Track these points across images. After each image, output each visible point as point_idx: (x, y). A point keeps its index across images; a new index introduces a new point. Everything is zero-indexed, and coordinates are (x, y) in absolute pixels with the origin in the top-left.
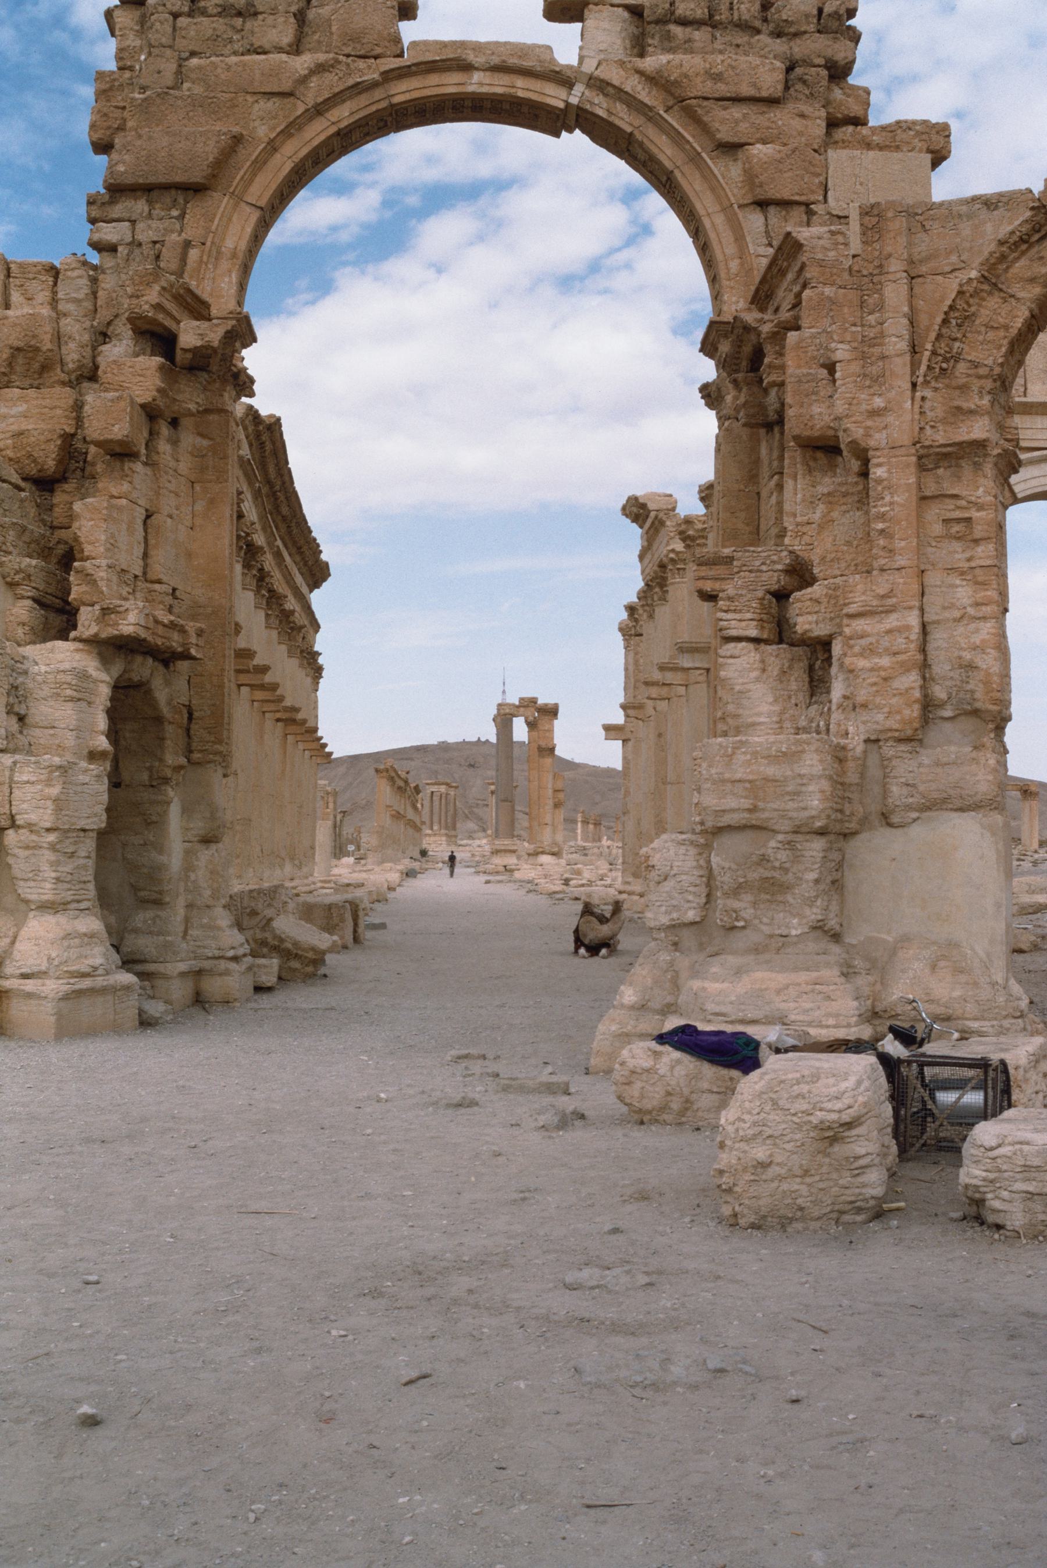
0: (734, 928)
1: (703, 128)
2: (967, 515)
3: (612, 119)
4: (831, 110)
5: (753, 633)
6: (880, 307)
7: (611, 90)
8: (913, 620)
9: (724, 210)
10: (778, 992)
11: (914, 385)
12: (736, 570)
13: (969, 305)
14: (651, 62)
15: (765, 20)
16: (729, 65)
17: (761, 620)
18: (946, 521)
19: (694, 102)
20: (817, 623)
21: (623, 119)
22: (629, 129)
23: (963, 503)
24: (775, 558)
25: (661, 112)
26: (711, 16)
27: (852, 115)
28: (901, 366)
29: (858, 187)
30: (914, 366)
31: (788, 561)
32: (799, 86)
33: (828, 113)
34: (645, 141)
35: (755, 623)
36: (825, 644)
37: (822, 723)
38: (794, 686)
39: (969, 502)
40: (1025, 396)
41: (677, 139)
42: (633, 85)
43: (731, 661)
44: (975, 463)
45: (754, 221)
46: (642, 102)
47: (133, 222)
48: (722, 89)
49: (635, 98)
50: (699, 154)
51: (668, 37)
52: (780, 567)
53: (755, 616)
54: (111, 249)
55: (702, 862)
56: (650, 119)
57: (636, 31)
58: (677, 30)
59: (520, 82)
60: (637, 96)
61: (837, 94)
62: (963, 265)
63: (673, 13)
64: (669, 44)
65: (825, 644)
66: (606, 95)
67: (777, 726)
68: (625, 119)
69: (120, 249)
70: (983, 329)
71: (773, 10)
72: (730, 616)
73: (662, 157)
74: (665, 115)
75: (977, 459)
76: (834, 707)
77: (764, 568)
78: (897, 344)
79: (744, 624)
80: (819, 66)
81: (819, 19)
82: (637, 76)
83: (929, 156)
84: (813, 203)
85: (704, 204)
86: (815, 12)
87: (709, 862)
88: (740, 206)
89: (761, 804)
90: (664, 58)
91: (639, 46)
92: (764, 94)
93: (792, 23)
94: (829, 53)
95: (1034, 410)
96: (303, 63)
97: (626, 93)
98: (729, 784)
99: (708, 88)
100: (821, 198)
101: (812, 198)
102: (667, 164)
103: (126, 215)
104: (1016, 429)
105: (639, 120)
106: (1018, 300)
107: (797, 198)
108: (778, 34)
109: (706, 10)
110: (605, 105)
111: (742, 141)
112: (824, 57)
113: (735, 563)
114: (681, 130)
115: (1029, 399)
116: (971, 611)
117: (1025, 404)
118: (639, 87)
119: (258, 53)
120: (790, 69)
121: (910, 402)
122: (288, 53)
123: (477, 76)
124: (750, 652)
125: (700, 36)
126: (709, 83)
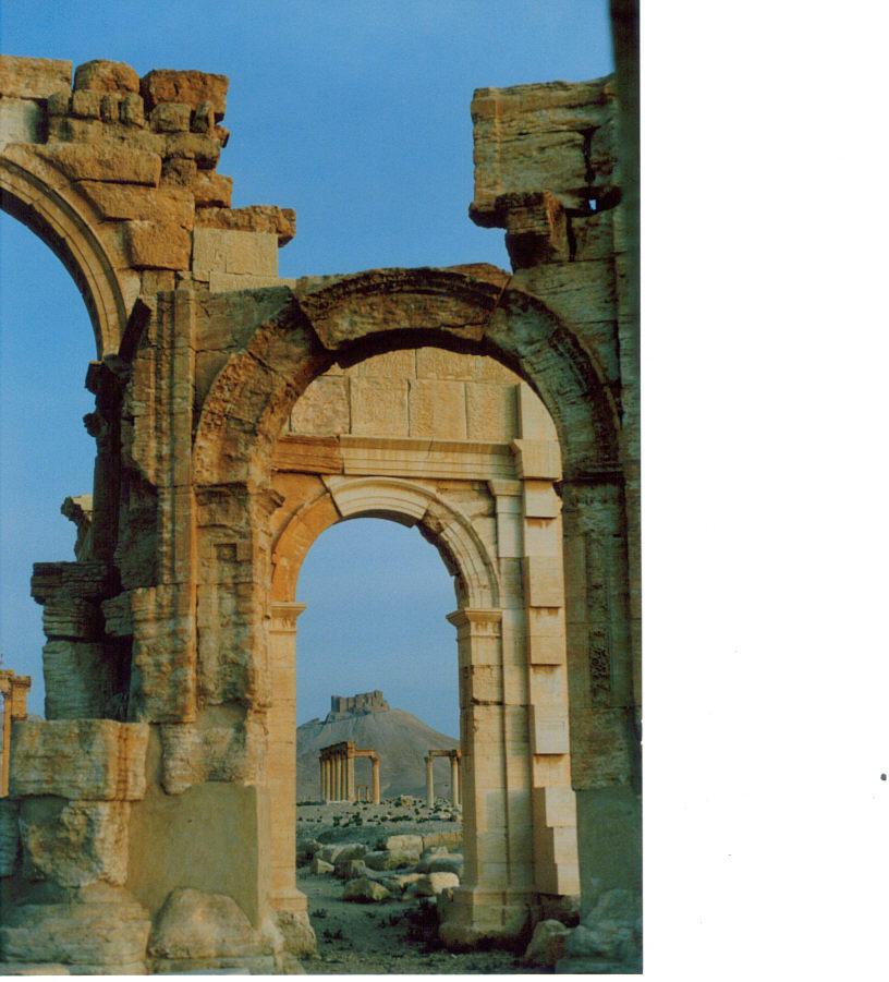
0: (36, 881)
1: (93, 205)
2: (233, 541)
3: (15, 192)
4: (199, 194)
5: (71, 633)
7: (16, 170)
9: (106, 273)
10: (64, 935)
12: (64, 580)
13: (239, 376)
15: (148, 119)
16: (115, 154)
17: (79, 622)
18: (218, 546)
19: (83, 183)
20: (120, 625)
21: (23, 193)
22: (29, 202)
23: (231, 532)
24: (95, 571)
25: (56, 190)
26: (102, 113)
27: (217, 199)
29: (218, 258)
31: (105, 574)
32: (174, 175)
33: (196, 197)
34: (43, 213)
35: (70, 625)
37: (121, 709)
38: (104, 677)
39: (235, 531)
40: (350, 433)
41: (70, 213)
42: (35, 166)
43: (53, 656)
44: (239, 500)
46: (40, 181)
48: (110, 175)
49: (35, 177)
50: (86, 226)
51: (66, 129)
52: (98, 578)
53: (73, 619)
55: (13, 826)
56: (46, 194)
57: (41, 120)
58: (76, 125)
60: (38, 175)
61: (204, 181)
62: (235, 344)
64: (67, 133)
66: (11, 173)
67: (87, 710)
68: (26, 193)
70: (249, 395)
71: (154, 111)
73: (55, 226)
74: (60, 193)
75: (241, 497)
76: (131, 695)
77: (86, 579)
79: (65, 625)
80: (190, 159)
82: (38, 159)
83: (277, 236)
84: (181, 270)
85: (91, 267)
86: (188, 115)
87: (17, 825)
89: (57, 777)
90: (62, 146)
91: (41, 131)
92: (142, 180)
93: (170, 123)
94: (198, 148)
95: (356, 444)
97: (27, 172)
98: (15, 760)
99: (98, 173)
100: (187, 266)
101: (179, 266)
102: (62, 235)
104: (342, 459)
105: (38, 195)
106: (275, 372)
107: (166, 265)
108: (159, 130)
109: (98, 109)
110: (9, 181)
111: (123, 216)
112: (195, 153)
113: (64, 574)
114: (72, 205)
115: (353, 436)
116: (234, 618)
117: (349, 440)
118: (40, 168)
120: (166, 160)
121: (190, 450)
124: (67, 648)
125: (94, 128)
126: (98, 169)
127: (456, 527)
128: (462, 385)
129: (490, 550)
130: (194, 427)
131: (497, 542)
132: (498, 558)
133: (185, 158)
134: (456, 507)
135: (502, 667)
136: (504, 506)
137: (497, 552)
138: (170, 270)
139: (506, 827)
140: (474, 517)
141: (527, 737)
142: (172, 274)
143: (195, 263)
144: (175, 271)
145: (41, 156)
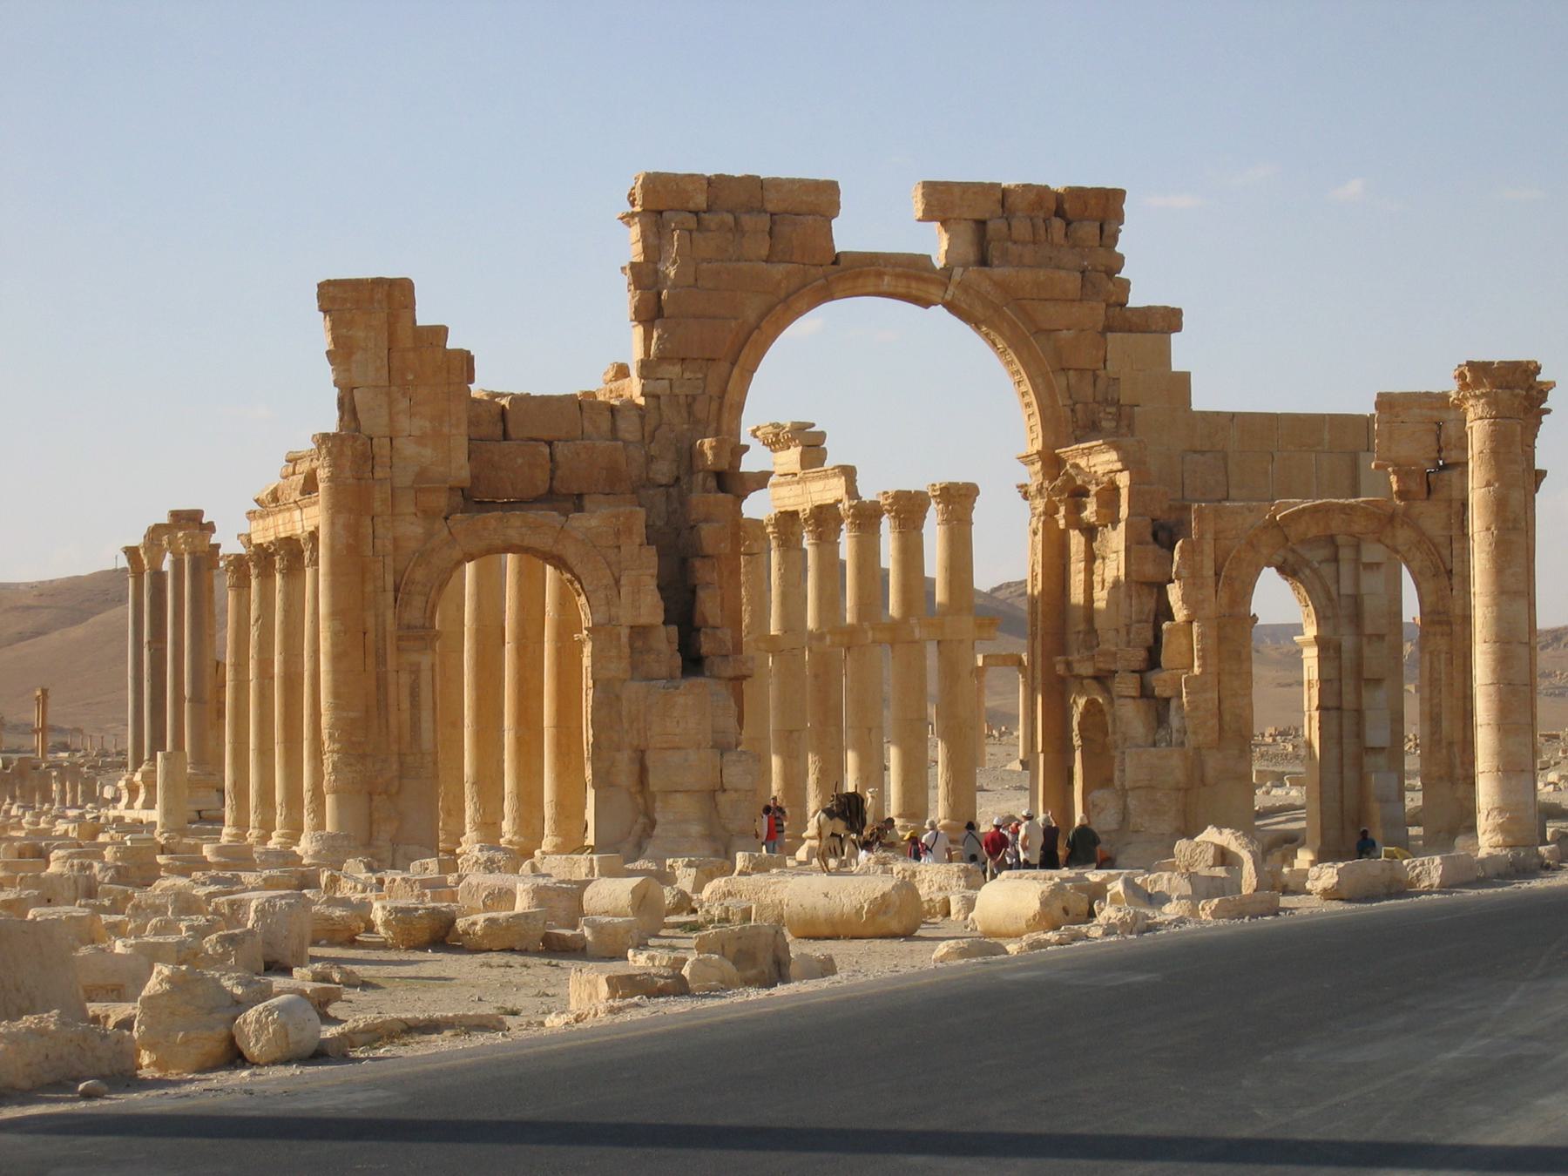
5: (1134, 694)
6: (1202, 552)
8: (1216, 696)
11: (1216, 591)
14: (998, 272)
19: (1024, 302)
28: (1211, 581)
30: (1217, 585)
36: (1168, 700)
42: (986, 286)
45: (1062, 381)
47: (671, 380)
54: (657, 397)
59: (914, 284)
63: (1010, 235)
65: (1168, 700)
69: (662, 398)
72: (1121, 686)
78: (1209, 572)
80: (1101, 272)
81: (1101, 238)
88: (1053, 372)
96: (778, 270)
103: (667, 376)
119: (746, 261)
122: (766, 261)
123: (886, 279)
127: (1307, 572)
128: (1314, 455)
129: (1333, 589)
130: (1217, 585)
131: (1338, 582)
132: (1339, 594)
133: (1097, 271)
134: (1308, 555)
135: (1340, 680)
136: (1346, 554)
137: (1338, 589)
138: (1089, 370)
139: (1342, 802)
140: (1320, 563)
141: (1359, 735)
142: (1091, 373)
143: (1108, 363)
144: (1094, 371)
145: (991, 279)
